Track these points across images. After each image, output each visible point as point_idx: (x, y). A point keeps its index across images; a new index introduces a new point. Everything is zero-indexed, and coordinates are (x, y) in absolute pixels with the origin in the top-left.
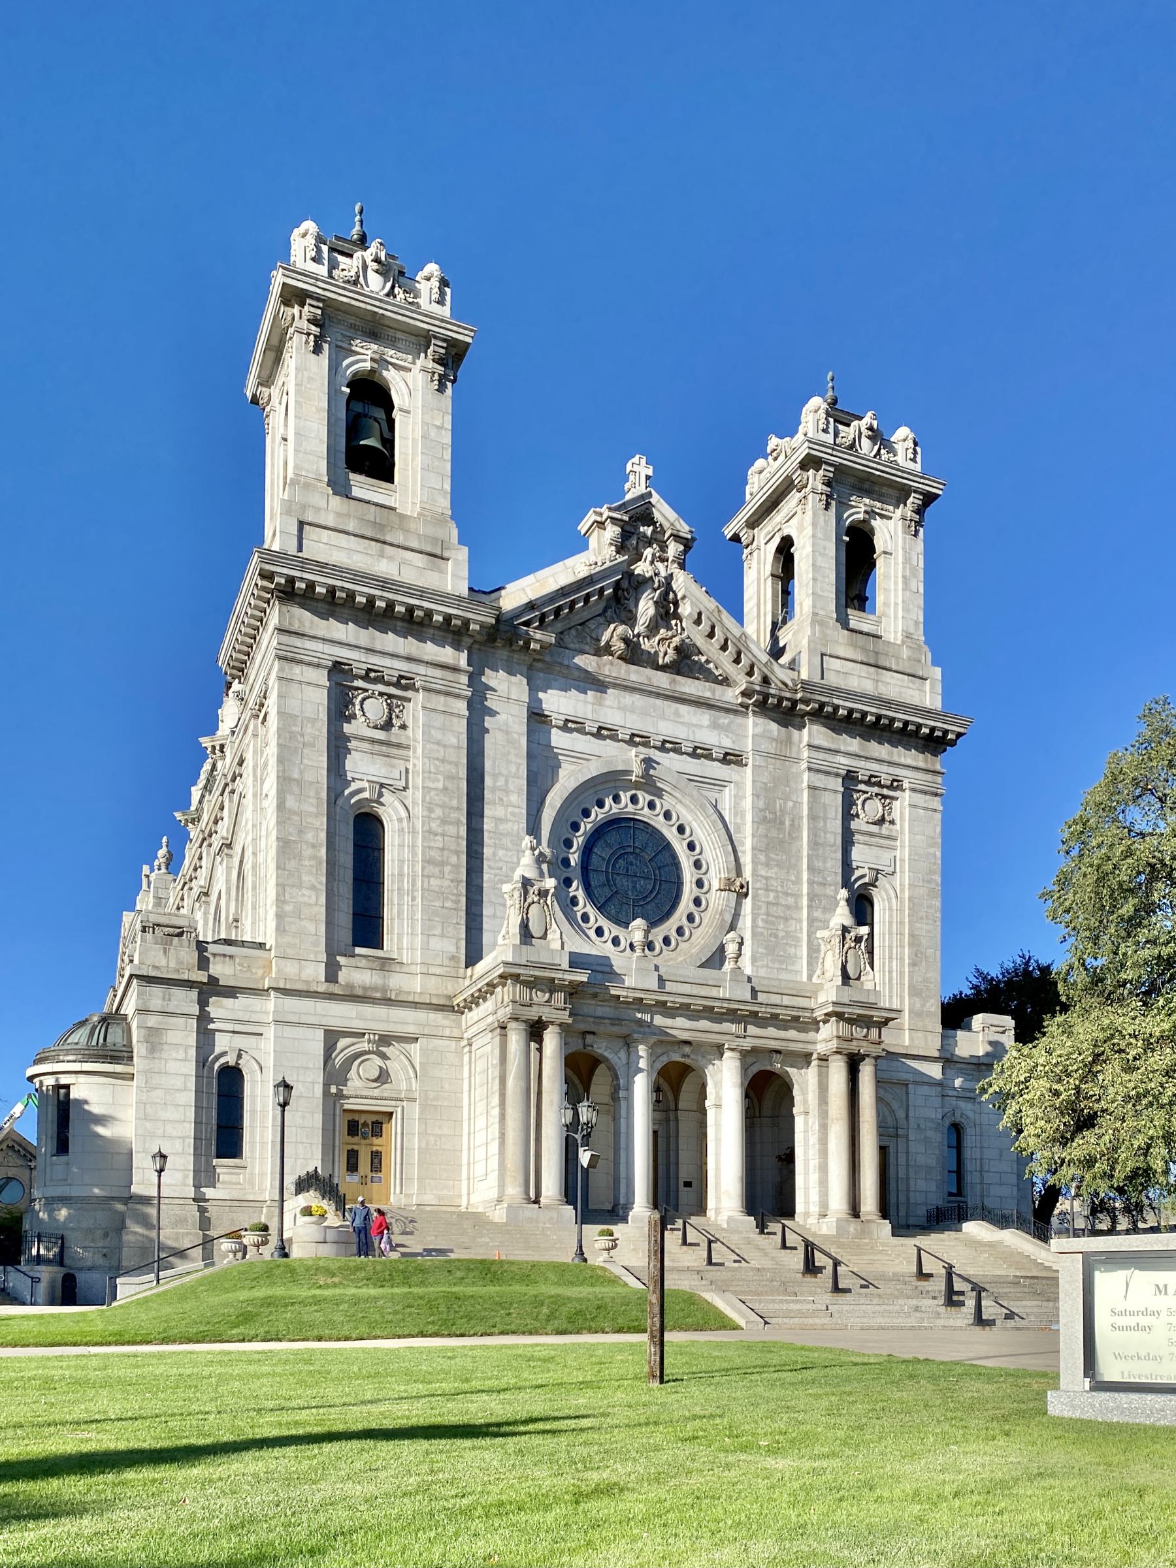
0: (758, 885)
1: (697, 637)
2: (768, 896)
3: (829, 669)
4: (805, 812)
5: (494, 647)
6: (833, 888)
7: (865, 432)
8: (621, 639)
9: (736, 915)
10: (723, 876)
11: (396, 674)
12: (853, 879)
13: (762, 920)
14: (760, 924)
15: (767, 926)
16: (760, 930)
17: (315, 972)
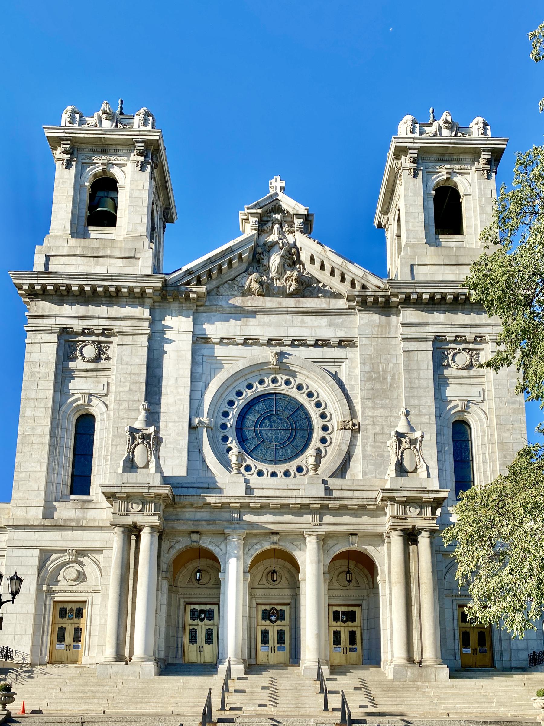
0: (366, 422)
1: (313, 270)
2: (375, 429)
3: (418, 273)
4: (402, 366)
5: (169, 303)
6: (427, 417)
7: (443, 126)
8: (256, 281)
9: (352, 445)
10: (340, 420)
11: (101, 328)
12: (448, 408)
13: (370, 446)
14: (369, 448)
15: (374, 450)
16: (369, 453)
17: (40, 512)
